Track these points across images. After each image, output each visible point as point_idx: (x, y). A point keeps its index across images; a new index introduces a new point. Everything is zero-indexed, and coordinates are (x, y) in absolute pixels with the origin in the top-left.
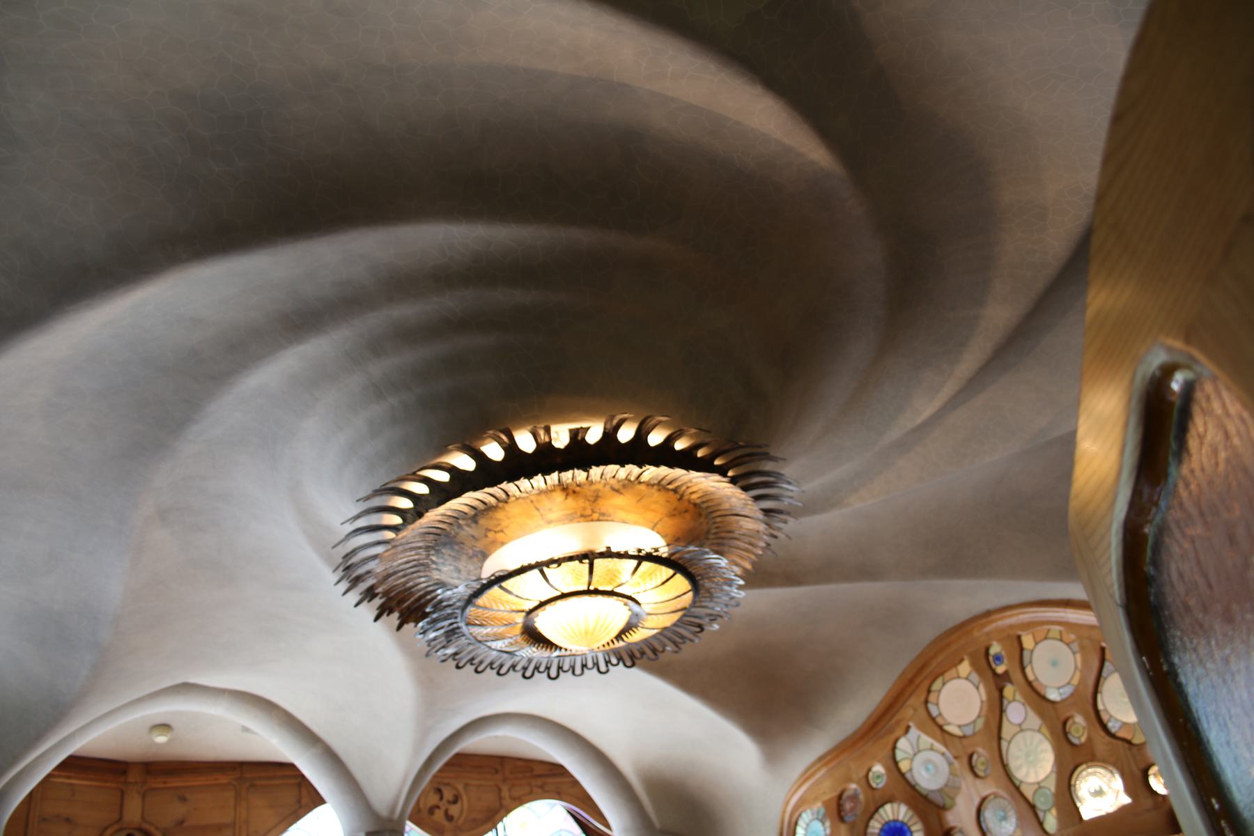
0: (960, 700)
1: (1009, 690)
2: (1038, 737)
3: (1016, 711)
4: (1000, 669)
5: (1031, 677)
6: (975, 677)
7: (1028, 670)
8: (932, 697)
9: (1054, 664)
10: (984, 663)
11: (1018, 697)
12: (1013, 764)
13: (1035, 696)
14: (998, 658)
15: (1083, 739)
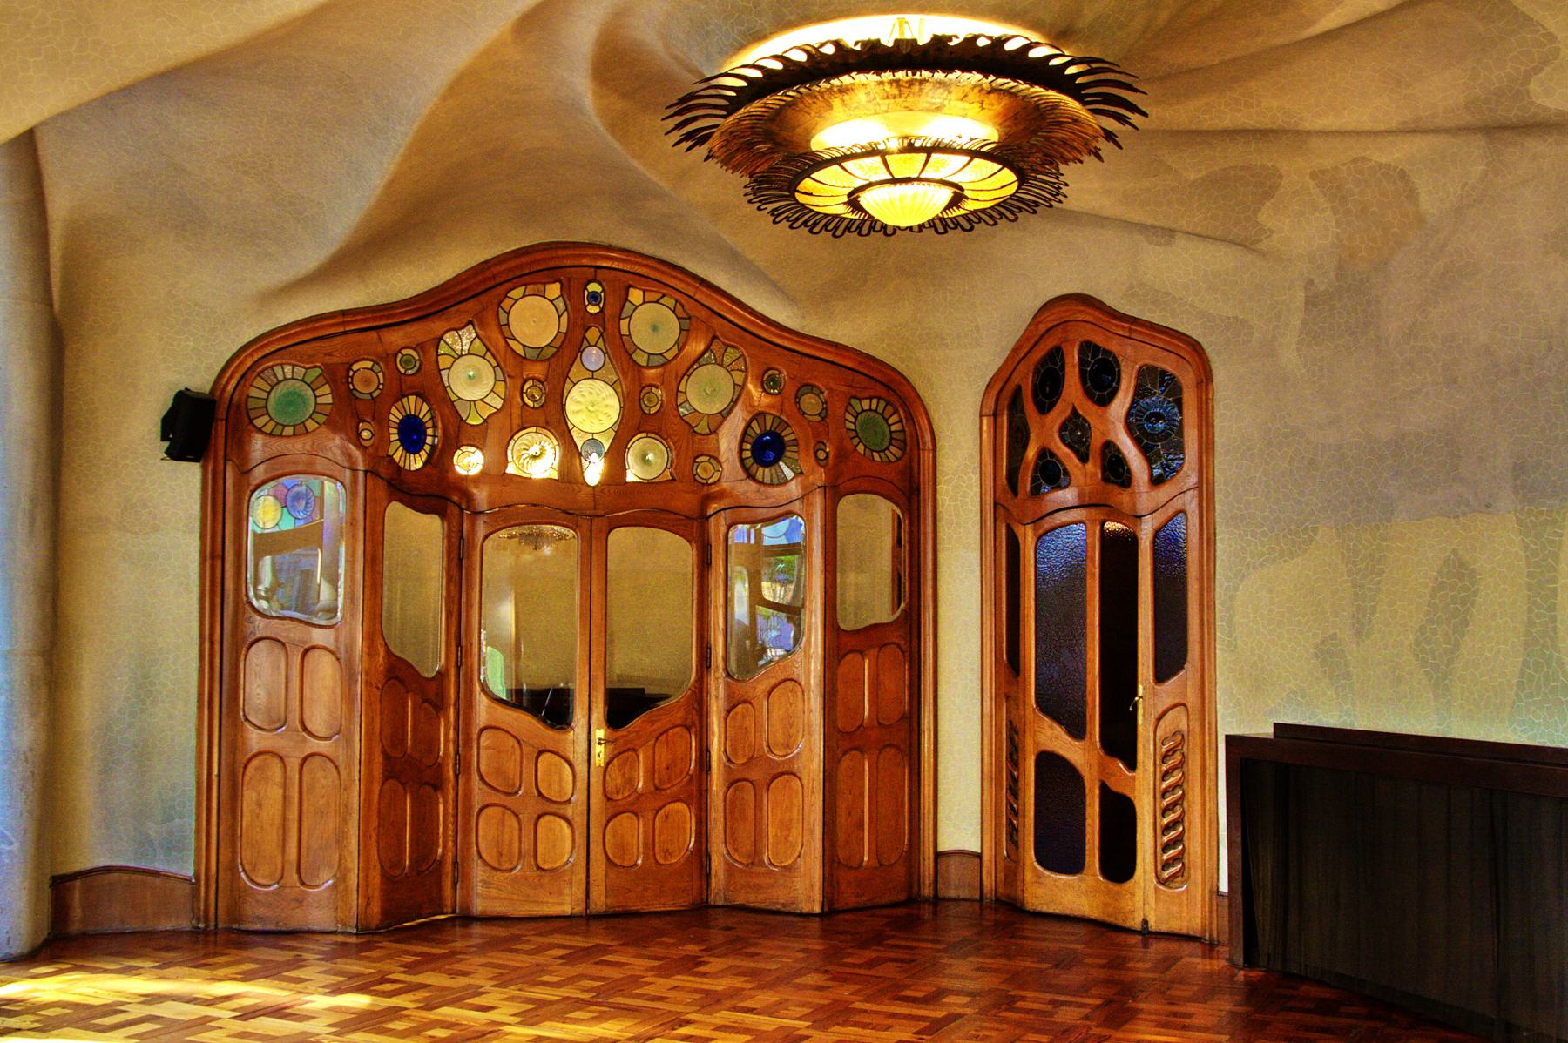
0: (535, 318)
1: (593, 334)
2: (612, 392)
3: (593, 357)
4: (593, 309)
5: (624, 331)
6: (561, 304)
7: (624, 323)
8: (506, 304)
9: (655, 328)
10: (573, 297)
11: (601, 343)
12: (570, 407)
13: (622, 353)
14: (594, 297)
15: (653, 411)
